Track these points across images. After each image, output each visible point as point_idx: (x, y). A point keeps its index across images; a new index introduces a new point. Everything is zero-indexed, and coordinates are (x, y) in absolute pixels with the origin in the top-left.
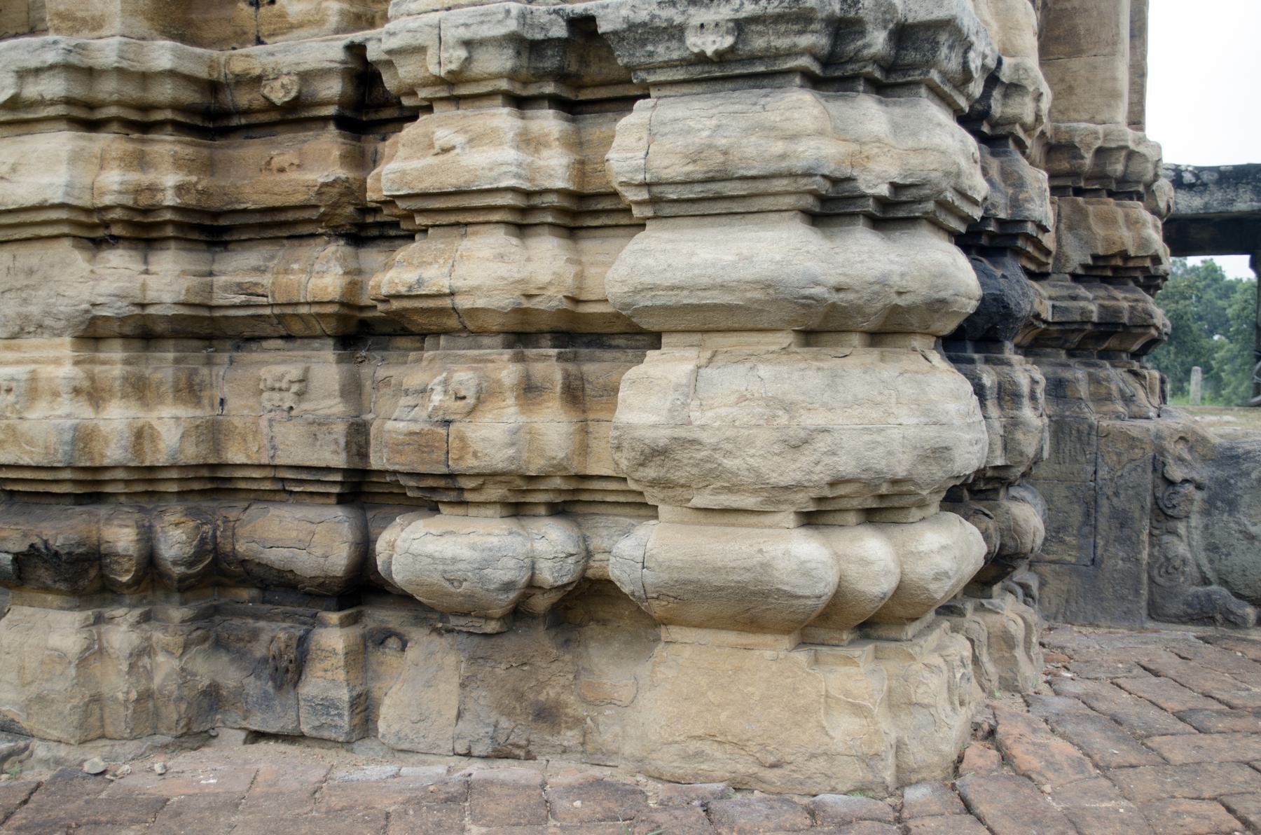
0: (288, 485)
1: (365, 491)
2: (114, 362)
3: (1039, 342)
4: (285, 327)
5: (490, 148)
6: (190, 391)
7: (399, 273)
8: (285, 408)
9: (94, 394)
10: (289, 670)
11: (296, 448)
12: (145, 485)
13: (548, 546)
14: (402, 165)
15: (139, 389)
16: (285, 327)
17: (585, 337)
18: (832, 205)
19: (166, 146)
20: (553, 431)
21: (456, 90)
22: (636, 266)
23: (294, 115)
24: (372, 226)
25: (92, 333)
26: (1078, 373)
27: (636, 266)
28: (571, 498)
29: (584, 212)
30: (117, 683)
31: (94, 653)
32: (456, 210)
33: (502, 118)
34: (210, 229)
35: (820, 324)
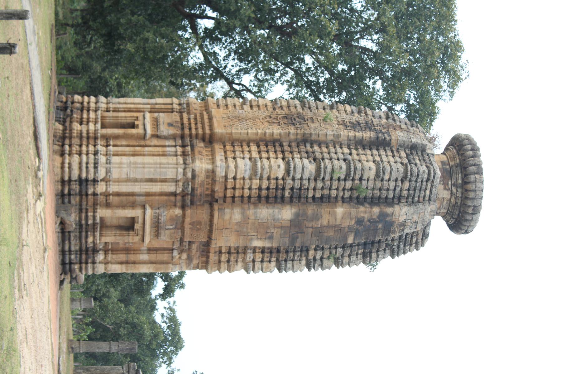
0: (70, 141)
2: (79, 132)
6: (77, 136)
8: (76, 141)
9: (77, 130)
13: (67, 152)
15: (77, 133)
17: (80, 154)
18: (87, 163)
19: (93, 135)
20: (74, 152)
22: (84, 157)
23: (95, 142)
25: (81, 131)
29: (87, 154)
30: (58, 131)
31: (59, 130)
33: (93, 150)
34: (88, 138)
35: (80, 163)
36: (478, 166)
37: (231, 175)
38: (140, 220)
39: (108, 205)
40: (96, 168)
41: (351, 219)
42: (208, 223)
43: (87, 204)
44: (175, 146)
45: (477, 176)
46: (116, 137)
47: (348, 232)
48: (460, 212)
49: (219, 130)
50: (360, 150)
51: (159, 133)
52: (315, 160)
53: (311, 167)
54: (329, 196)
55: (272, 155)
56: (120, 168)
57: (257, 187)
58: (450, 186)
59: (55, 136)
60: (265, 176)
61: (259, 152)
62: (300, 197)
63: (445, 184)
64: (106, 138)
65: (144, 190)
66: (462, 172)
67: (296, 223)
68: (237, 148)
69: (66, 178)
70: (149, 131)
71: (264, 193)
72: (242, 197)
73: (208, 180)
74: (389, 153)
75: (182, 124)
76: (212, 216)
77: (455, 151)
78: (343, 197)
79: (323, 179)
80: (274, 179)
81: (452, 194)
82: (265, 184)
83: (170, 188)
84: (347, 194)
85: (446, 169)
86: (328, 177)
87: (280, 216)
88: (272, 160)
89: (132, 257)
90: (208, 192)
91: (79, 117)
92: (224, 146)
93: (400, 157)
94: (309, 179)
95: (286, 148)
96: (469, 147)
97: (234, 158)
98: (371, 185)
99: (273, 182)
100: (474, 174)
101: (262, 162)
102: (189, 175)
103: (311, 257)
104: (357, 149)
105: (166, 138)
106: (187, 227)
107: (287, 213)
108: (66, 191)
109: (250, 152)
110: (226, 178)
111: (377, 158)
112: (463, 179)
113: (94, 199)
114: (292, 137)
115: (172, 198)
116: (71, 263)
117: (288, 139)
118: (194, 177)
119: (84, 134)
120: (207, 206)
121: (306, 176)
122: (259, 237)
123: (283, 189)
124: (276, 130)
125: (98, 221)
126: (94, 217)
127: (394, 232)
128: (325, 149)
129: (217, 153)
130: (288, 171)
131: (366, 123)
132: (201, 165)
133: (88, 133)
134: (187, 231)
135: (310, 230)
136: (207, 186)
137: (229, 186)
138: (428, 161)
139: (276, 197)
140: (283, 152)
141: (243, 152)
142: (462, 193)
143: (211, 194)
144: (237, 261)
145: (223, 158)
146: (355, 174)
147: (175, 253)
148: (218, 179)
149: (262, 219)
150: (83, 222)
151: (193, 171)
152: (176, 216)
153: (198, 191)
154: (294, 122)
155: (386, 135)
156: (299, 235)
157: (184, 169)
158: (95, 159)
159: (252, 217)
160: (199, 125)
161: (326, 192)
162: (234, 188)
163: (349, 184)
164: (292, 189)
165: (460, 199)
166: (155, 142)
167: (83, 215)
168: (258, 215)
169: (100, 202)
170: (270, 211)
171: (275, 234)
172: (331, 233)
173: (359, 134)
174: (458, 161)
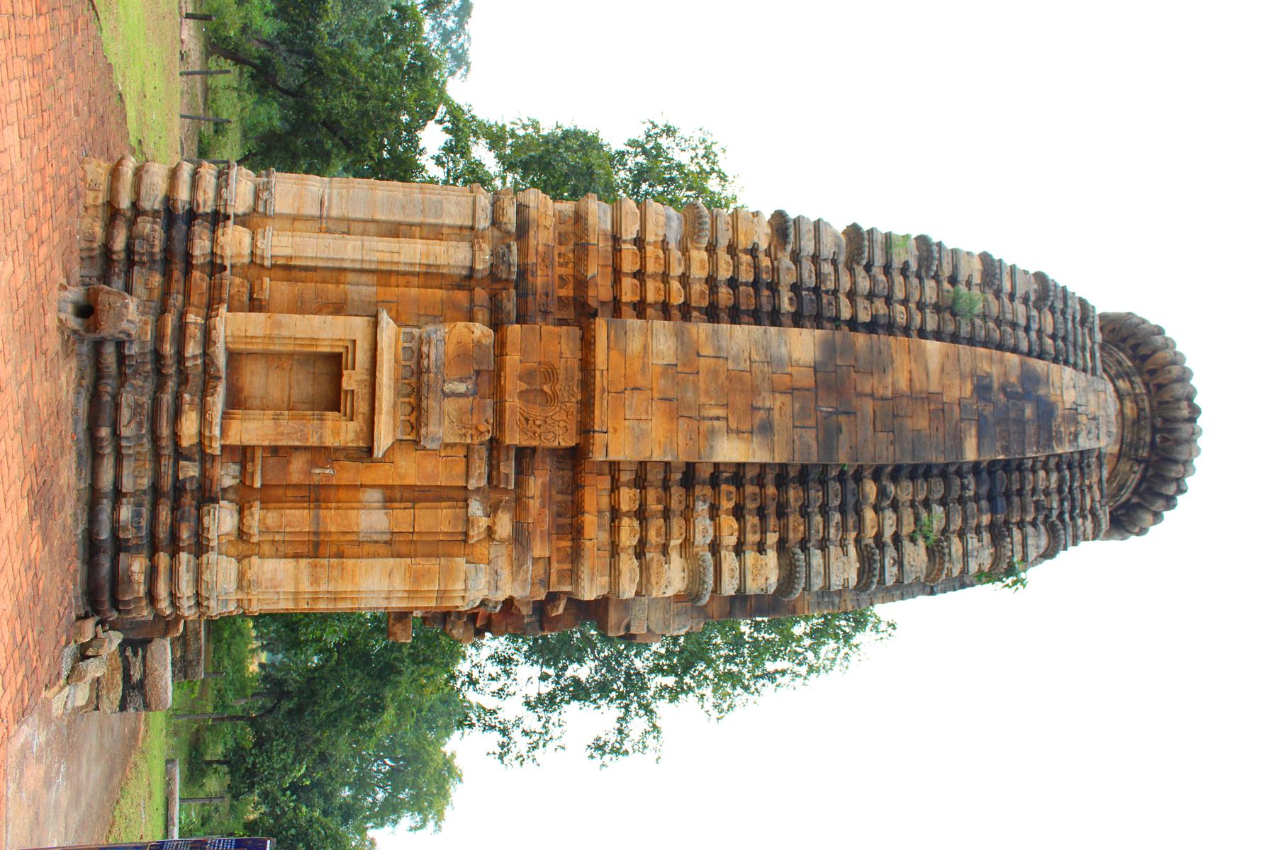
38: (362, 357)
39: (255, 305)
42: (578, 375)
47: (962, 420)
48: (1155, 430)
57: (704, 274)
60: (723, 242)
65: (376, 256)
66: (1121, 350)
67: (830, 379)
69: (125, 203)
71: (724, 293)
73: (563, 249)
76: (587, 343)
80: (746, 251)
83: (454, 256)
86: (879, 261)
87: (784, 350)
89: (332, 520)
90: (567, 292)
99: (745, 258)
103: (870, 532)
106: (512, 385)
107: (802, 345)
108: (119, 243)
110: (616, 239)
112: (1132, 359)
113: (211, 288)
115: (461, 296)
116: (119, 546)
122: (734, 426)
123: (773, 288)
134: (513, 403)
135: (868, 405)
136: (562, 271)
137: (628, 265)
142: (1146, 385)
143: (575, 298)
144: (665, 550)
147: (476, 508)
148: (593, 240)
149: (736, 359)
150: (168, 349)
152: (478, 344)
153: (539, 280)
156: (842, 418)
159: (707, 350)
162: (640, 275)
165: (1145, 398)
167: (170, 320)
168: (724, 343)
169: (231, 297)
171: (776, 415)
172: (922, 423)
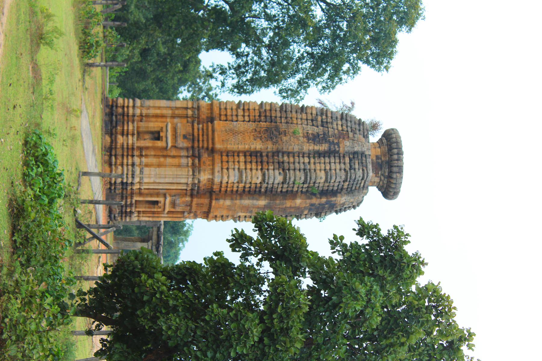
0: (116, 152)
1: (116, 156)
3: (122, 193)
4: (123, 152)
5: (130, 161)
7: (125, 158)
10: (107, 151)
11: (117, 152)
12: (116, 145)
13: (114, 163)
14: (130, 157)
16: (123, 152)
17: (122, 165)
18: (127, 174)
21: (132, 160)
22: (125, 168)
23: (133, 153)
24: (127, 156)
25: (123, 143)
26: (120, 195)
27: (125, 168)
28: (115, 164)
29: (127, 165)
32: (128, 159)
34: (128, 148)
36: (400, 168)
37: (224, 181)
38: (162, 202)
39: (140, 194)
40: (133, 177)
41: (306, 204)
43: (127, 193)
44: (187, 157)
45: (398, 175)
46: (147, 148)
49: (218, 146)
50: (316, 159)
51: (176, 145)
52: (283, 170)
53: (279, 179)
54: (292, 191)
55: (254, 167)
56: (149, 177)
58: (380, 175)
59: (105, 147)
61: (245, 162)
62: (272, 191)
63: (376, 174)
64: (141, 149)
68: (231, 159)
69: (113, 182)
70: (170, 145)
72: (232, 190)
74: (337, 161)
75: (193, 135)
77: (387, 149)
78: (302, 191)
79: (288, 183)
81: (381, 180)
82: (248, 186)
84: (304, 190)
85: (379, 163)
88: (254, 171)
91: (121, 129)
92: (222, 156)
93: (344, 163)
94: (278, 184)
95: (265, 159)
96: (395, 151)
97: (228, 169)
98: (321, 185)
100: (397, 173)
101: (246, 173)
102: (196, 182)
104: (314, 158)
105: (182, 149)
107: (262, 202)
109: (239, 162)
111: (328, 168)
112: (388, 174)
114: (269, 150)
115: (185, 191)
117: (266, 151)
118: (199, 182)
119: (125, 146)
120: (208, 195)
121: (276, 182)
123: (261, 187)
124: (258, 146)
125: (134, 202)
126: (131, 201)
127: (337, 207)
128: (292, 160)
129: (216, 165)
130: (264, 180)
131: (324, 134)
132: (204, 177)
133: (128, 145)
135: (278, 209)
138: (364, 164)
139: (255, 191)
140: (262, 162)
141: (234, 162)
145: (220, 170)
146: (310, 181)
147: (186, 214)
151: (199, 179)
154: (272, 135)
155: (336, 146)
157: (193, 178)
158: (133, 171)
160: (205, 137)
161: (290, 189)
163: (306, 186)
164: (267, 188)
166: (174, 152)
170: (251, 201)
173: (317, 148)
174: (387, 158)
